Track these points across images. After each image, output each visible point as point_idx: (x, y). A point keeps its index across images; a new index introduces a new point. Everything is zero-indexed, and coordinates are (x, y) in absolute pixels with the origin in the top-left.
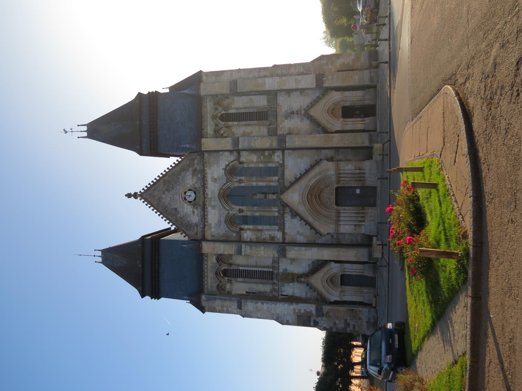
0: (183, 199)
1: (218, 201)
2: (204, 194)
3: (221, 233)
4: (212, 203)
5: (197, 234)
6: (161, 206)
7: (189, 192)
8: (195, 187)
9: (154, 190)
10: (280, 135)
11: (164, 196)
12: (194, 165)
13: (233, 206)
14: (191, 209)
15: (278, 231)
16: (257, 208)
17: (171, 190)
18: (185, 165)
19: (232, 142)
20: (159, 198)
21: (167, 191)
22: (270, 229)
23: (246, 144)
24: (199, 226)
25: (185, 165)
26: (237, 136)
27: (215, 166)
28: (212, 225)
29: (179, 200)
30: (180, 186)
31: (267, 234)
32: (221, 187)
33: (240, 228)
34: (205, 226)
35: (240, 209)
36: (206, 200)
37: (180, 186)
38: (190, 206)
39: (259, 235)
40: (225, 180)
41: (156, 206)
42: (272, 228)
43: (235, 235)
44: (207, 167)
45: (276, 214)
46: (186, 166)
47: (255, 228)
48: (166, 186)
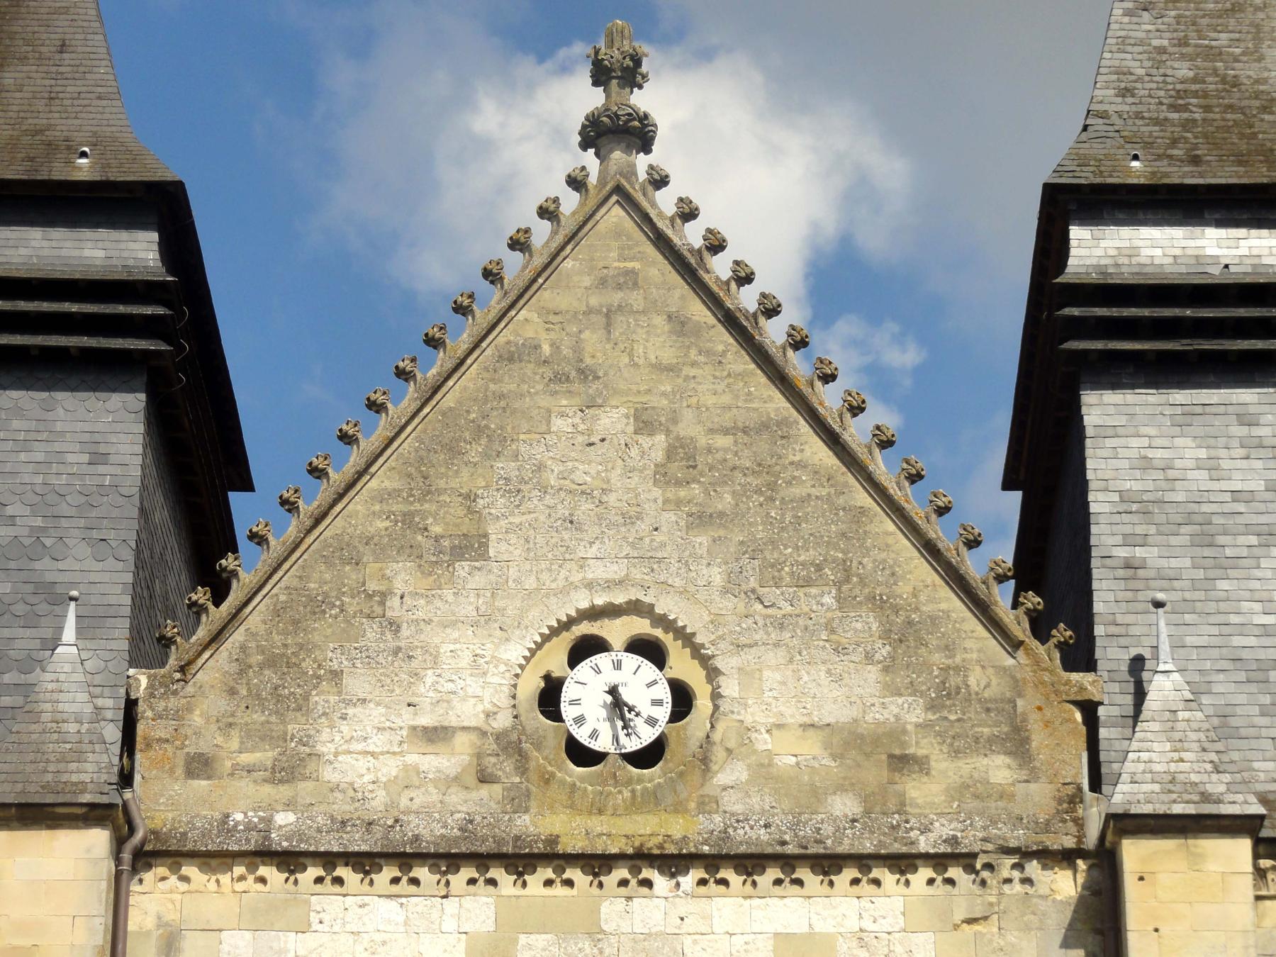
0: (585, 628)
2: (640, 858)
5: (200, 766)
6: (509, 386)
7: (664, 692)
8: (718, 754)
9: (680, 325)
11: (613, 420)
12: (956, 753)
14: (467, 713)
17: (678, 503)
18: (949, 649)
20: (586, 374)
21: (670, 454)
24: (285, 791)
25: (949, 649)
29: (570, 587)
30: (725, 591)
34: (290, 860)
36: (574, 873)
37: (725, 591)
38: (505, 702)
41: (504, 336)
44: (940, 889)
46: (938, 658)
48: (722, 441)
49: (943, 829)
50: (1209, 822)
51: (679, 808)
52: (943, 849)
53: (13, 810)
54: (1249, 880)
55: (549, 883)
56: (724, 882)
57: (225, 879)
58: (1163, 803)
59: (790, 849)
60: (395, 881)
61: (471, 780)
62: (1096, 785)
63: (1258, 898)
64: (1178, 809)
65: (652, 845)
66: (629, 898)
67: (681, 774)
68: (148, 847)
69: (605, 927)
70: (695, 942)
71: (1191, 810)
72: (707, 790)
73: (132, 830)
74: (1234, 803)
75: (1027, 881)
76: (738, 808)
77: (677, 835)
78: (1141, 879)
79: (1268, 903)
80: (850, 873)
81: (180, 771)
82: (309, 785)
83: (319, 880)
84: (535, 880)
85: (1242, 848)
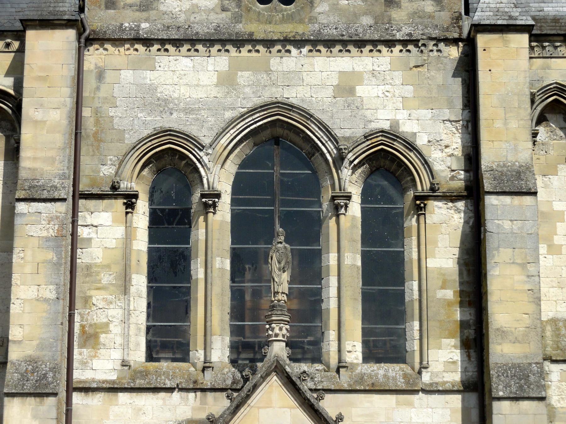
1: (257, 101)
3: (112, 112)
4: (246, 74)
10: (542, 374)
13: (232, 167)
15: (125, 364)
16: (222, 270)
19: (514, 164)
22: (132, 327)
23: (507, 225)
24: (144, 15)
26: (540, 182)
27: (409, 91)
28: (149, 74)
31: (111, 312)
32: (318, 115)
33: (136, 196)
34: (147, 42)
35: (218, 196)
36: (260, 47)
39: (106, 278)
40: (348, 133)
42: (133, 339)
43: (108, 171)
44: (405, 54)
45: (198, 355)
47: (134, 262)
49: (406, 30)
50: (512, 27)
51: (301, 21)
52: (406, 38)
53: (37, 22)
54: (527, 51)
55: (250, 51)
56: (319, 51)
57: (122, 49)
58: (494, 20)
59: (345, 38)
60: (189, 50)
61: (219, 10)
62: (467, 12)
63: (531, 58)
64: (500, 22)
65: (290, 36)
66: (281, 57)
67: (302, 8)
68: (91, 37)
69: (272, 69)
70: (307, 75)
71: (505, 22)
72: (313, 14)
73: (84, 30)
74: (522, 20)
75: (439, 51)
76: (325, 21)
77: (301, 32)
78: (484, 50)
79: (534, 60)
80: (369, 47)
81: (103, 7)
82: (154, 12)
83: (159, 50)
84: (244, 50)
85: (524, 38)
